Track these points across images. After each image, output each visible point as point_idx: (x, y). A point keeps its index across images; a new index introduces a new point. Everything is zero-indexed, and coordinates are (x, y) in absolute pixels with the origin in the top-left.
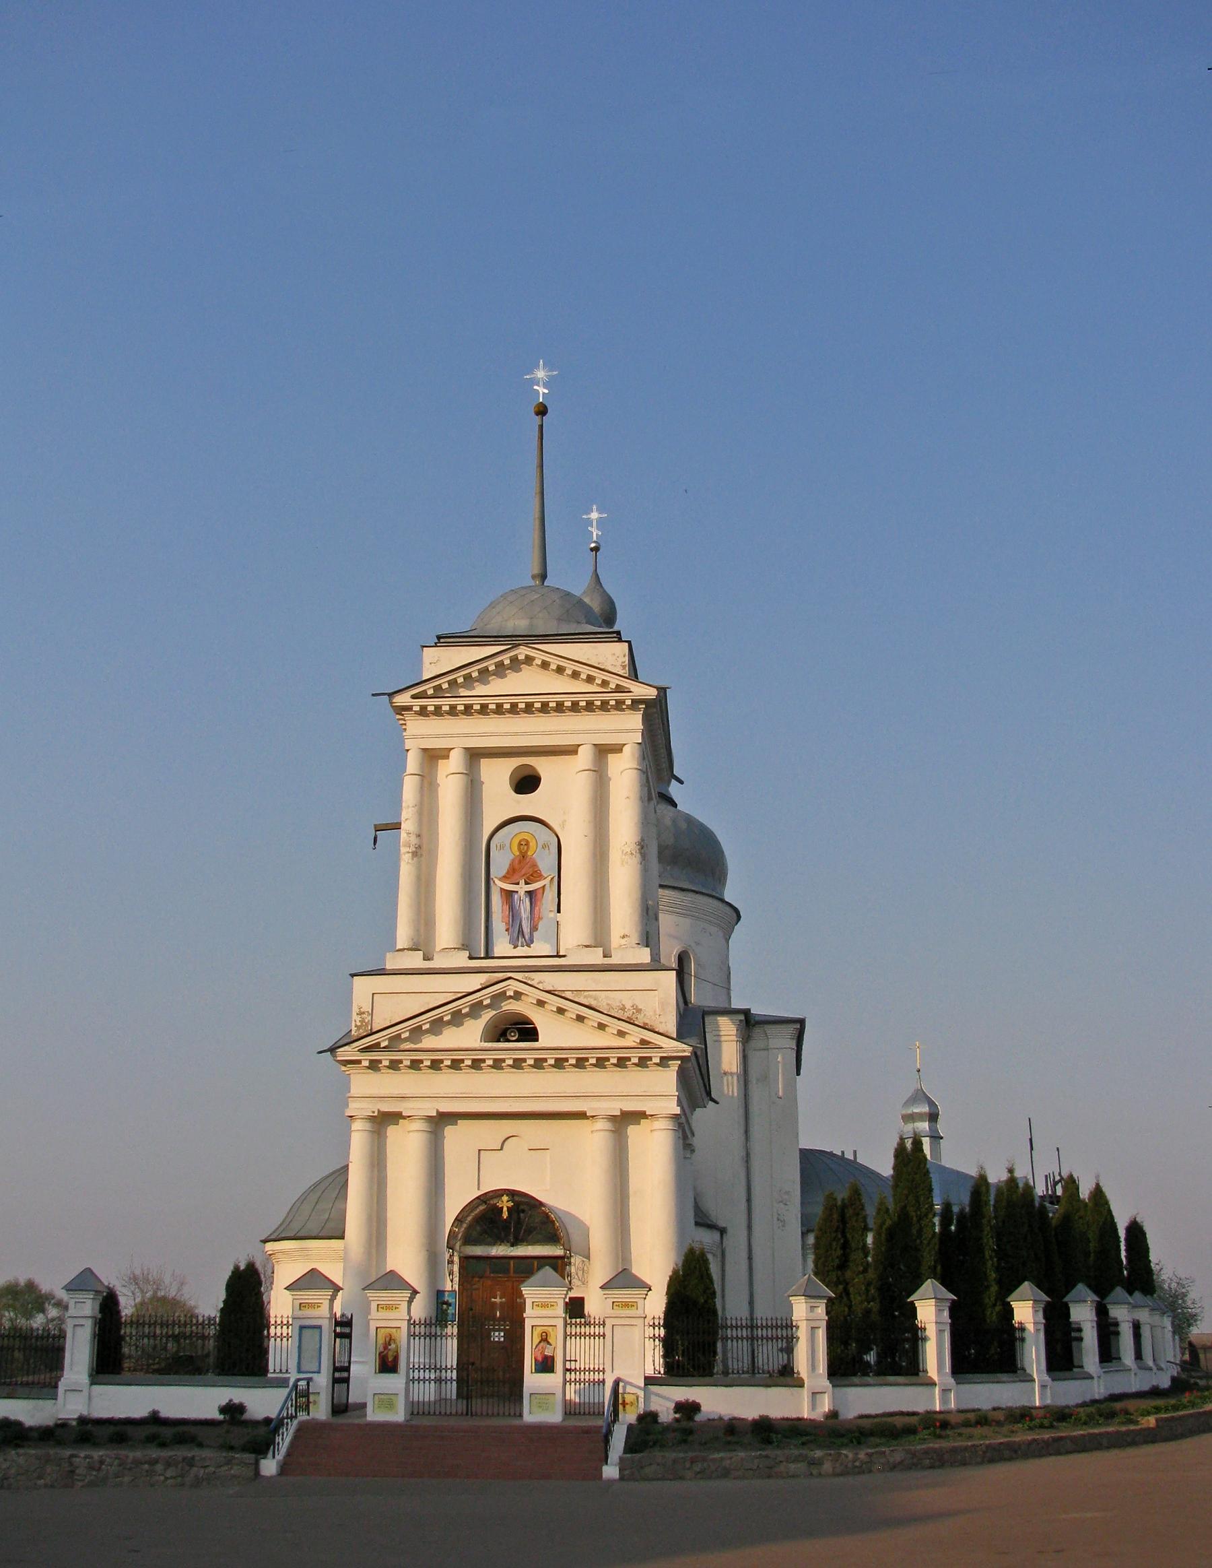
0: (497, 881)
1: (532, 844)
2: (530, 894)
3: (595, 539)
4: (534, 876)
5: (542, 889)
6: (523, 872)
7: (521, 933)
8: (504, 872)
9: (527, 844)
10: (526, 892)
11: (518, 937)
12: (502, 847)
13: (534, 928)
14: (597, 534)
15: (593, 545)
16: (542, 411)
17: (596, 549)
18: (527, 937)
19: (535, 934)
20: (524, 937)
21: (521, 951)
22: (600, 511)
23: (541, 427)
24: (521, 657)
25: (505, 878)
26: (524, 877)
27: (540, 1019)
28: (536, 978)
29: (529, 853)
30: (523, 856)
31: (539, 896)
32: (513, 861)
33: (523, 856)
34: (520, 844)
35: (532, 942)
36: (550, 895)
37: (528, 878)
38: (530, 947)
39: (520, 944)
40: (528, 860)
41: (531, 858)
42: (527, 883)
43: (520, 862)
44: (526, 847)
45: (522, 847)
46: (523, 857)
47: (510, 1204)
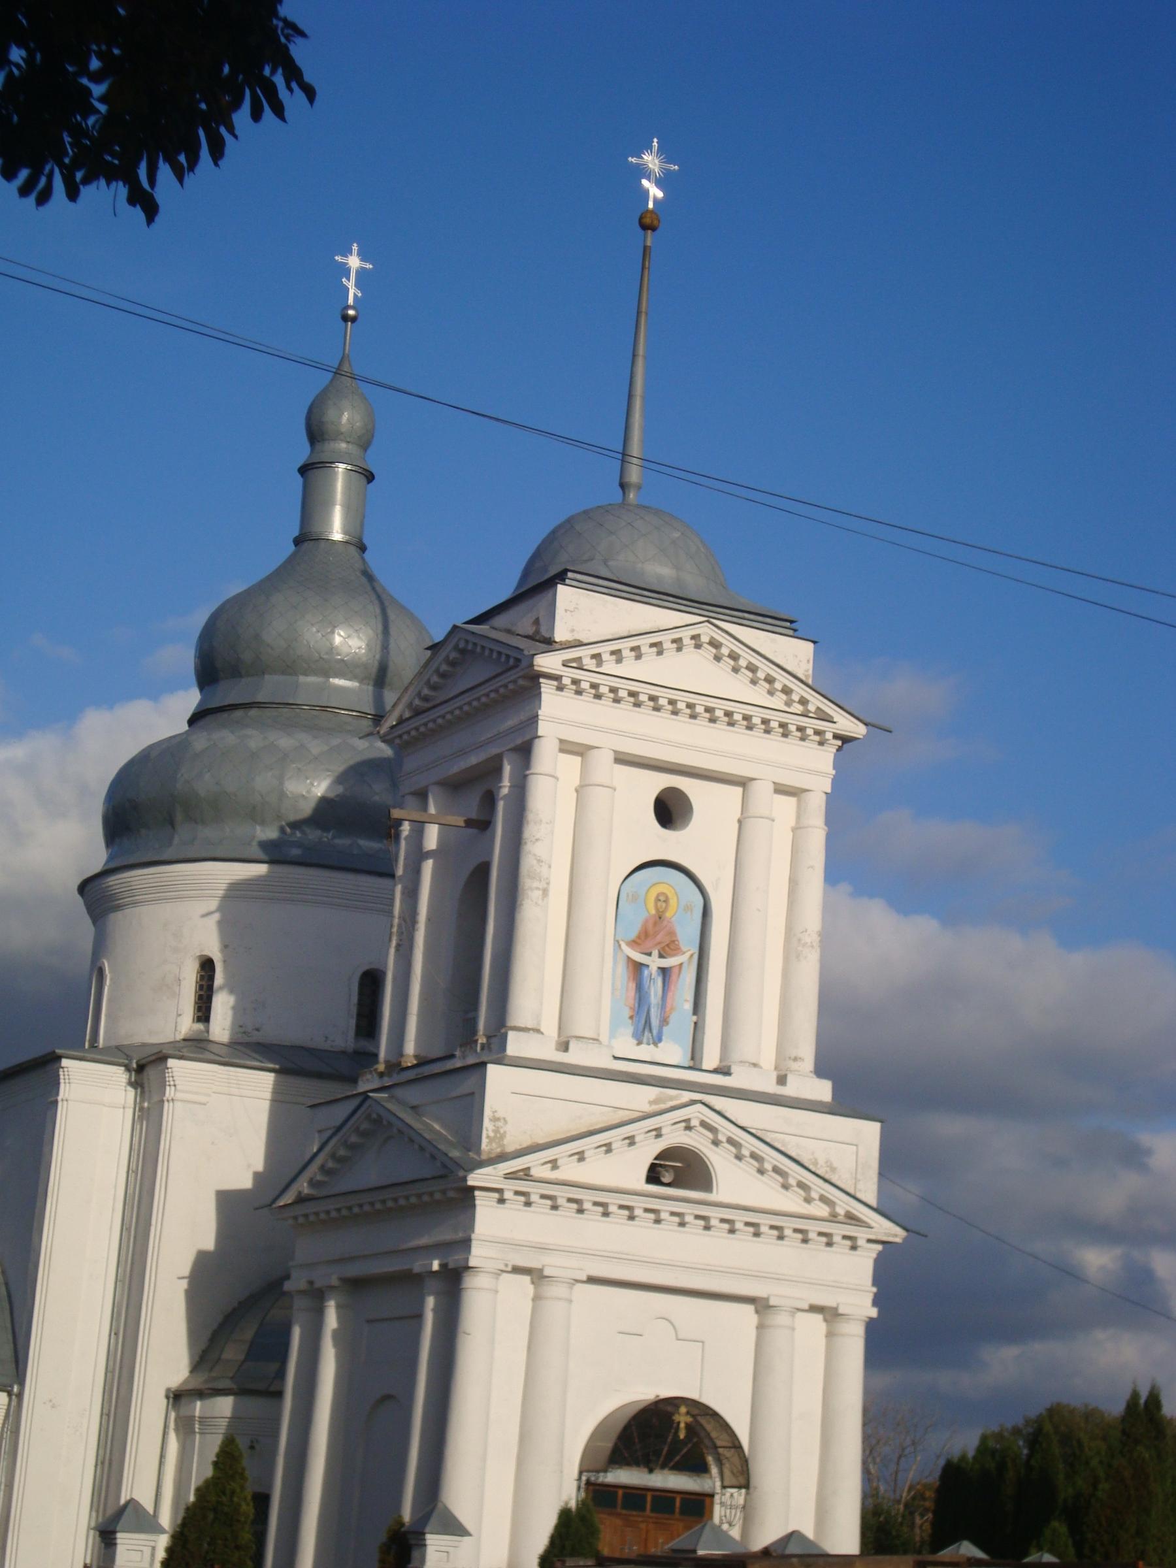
0: (624, 946)
1: (673, 902)
2: (664, 971)
3: (351, 301)
4: (669, 948)
5: (678, 967)
6: (659, 938)
7: (648, 1025)
8: (633, 935)
9: (666, 901)
10: (659, 968)
11: (644, 1029)
12: (634, 898)
13: (664, 1021)
14: (355, 295)
15: (351, 312)
16: (647, 225)
17: (354, 319)
18: (655, 1032)
19: (665, 1029)
20: (651, 1030)
21: (646, 1052)
22: (363, 256)
23: (646, 249)
24: (705, 639)
25: (634, 944)
26: (659, 947)
27: (719, 1161)
28: (718, 1102)
29: (668, 915)
30: (660, 917)
31: (674, 977)
32: (646, 921)
33: (660, 917)
34: (657, 900)
35: (660, 1040)
36: (688, 978)
37: (663, 948)
38: (657, 1047)
39: (645, 1040)
40: (665, 923)
41: (669, 922)
42: (661, 956)
43: (655, 924)
44: (664, 905)
45: (659, 904)
46: (660, 918)
47: (689, 1419)
